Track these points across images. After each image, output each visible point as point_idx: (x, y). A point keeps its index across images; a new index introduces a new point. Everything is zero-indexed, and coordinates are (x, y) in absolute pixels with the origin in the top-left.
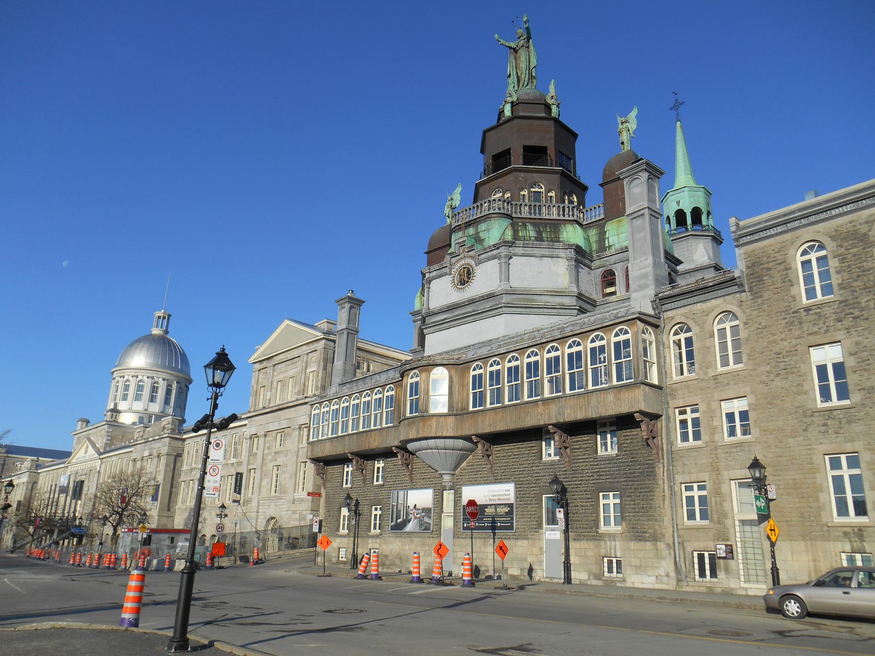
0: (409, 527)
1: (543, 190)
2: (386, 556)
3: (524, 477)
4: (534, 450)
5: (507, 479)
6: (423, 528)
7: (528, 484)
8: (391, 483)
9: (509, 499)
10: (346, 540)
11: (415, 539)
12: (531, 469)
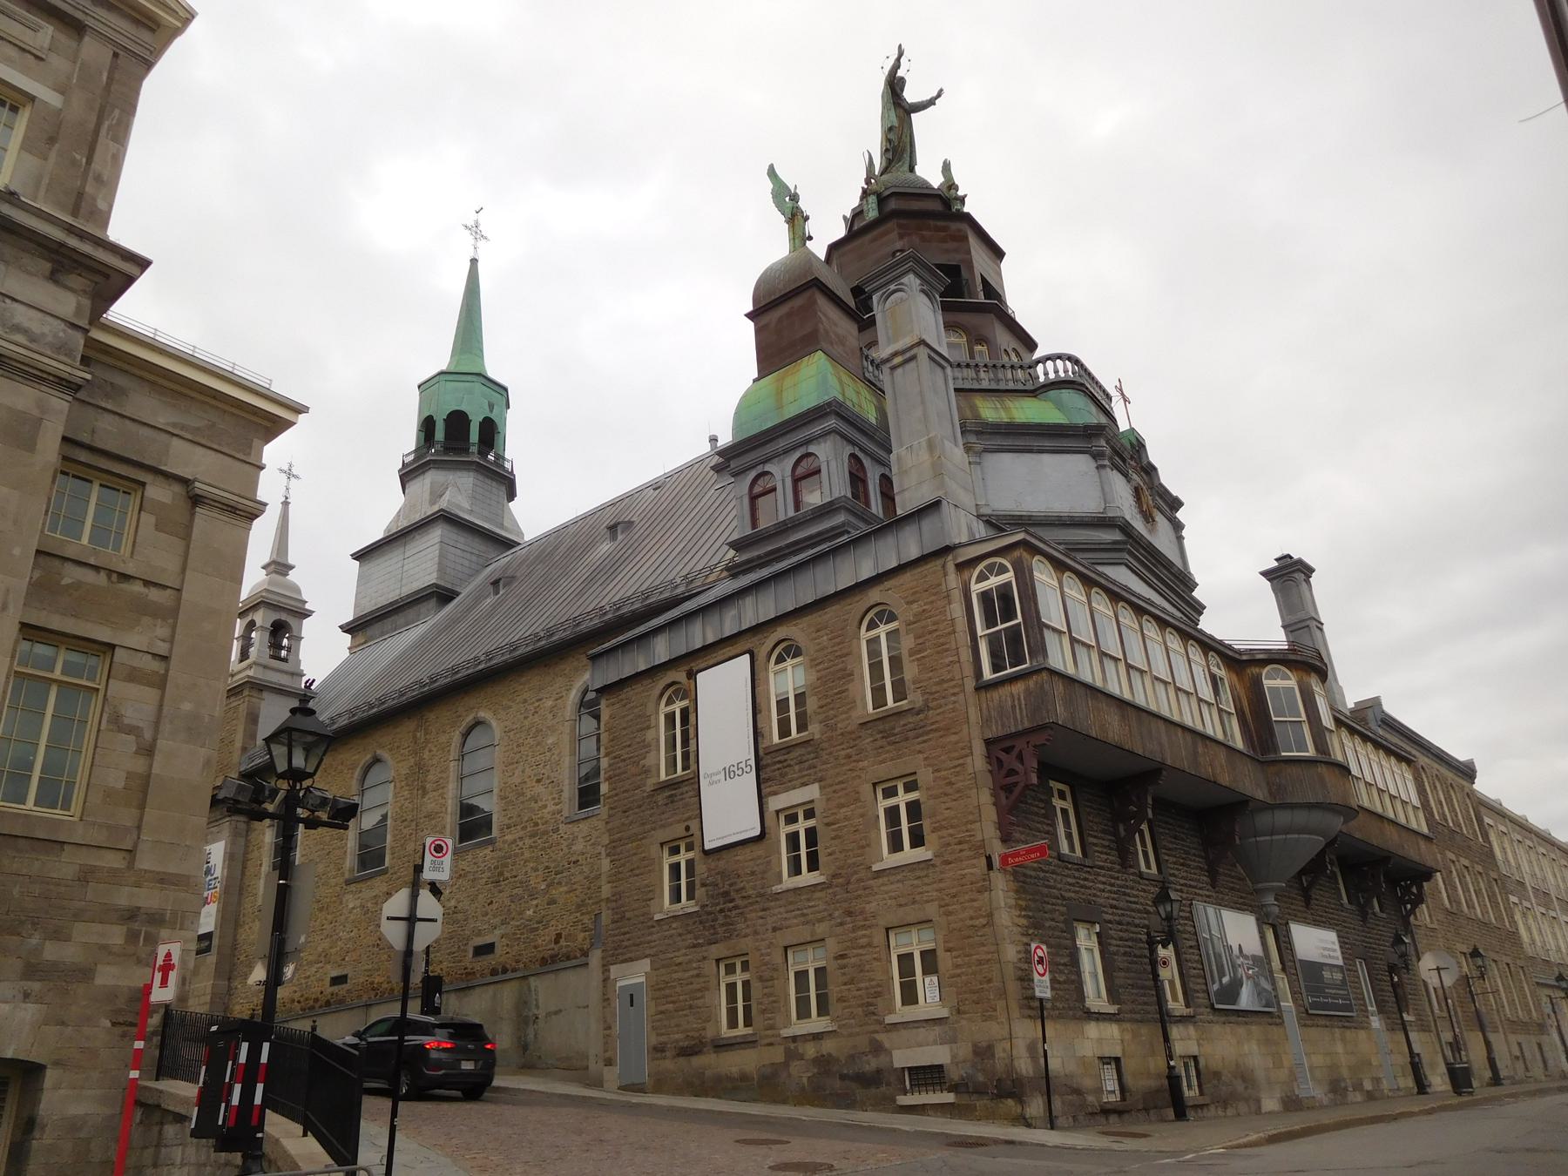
0: (1246, 1000)
2: (1217, 1075)
6: (1264, 1002)
8: (1182, 881)
10: (1113, 1030)
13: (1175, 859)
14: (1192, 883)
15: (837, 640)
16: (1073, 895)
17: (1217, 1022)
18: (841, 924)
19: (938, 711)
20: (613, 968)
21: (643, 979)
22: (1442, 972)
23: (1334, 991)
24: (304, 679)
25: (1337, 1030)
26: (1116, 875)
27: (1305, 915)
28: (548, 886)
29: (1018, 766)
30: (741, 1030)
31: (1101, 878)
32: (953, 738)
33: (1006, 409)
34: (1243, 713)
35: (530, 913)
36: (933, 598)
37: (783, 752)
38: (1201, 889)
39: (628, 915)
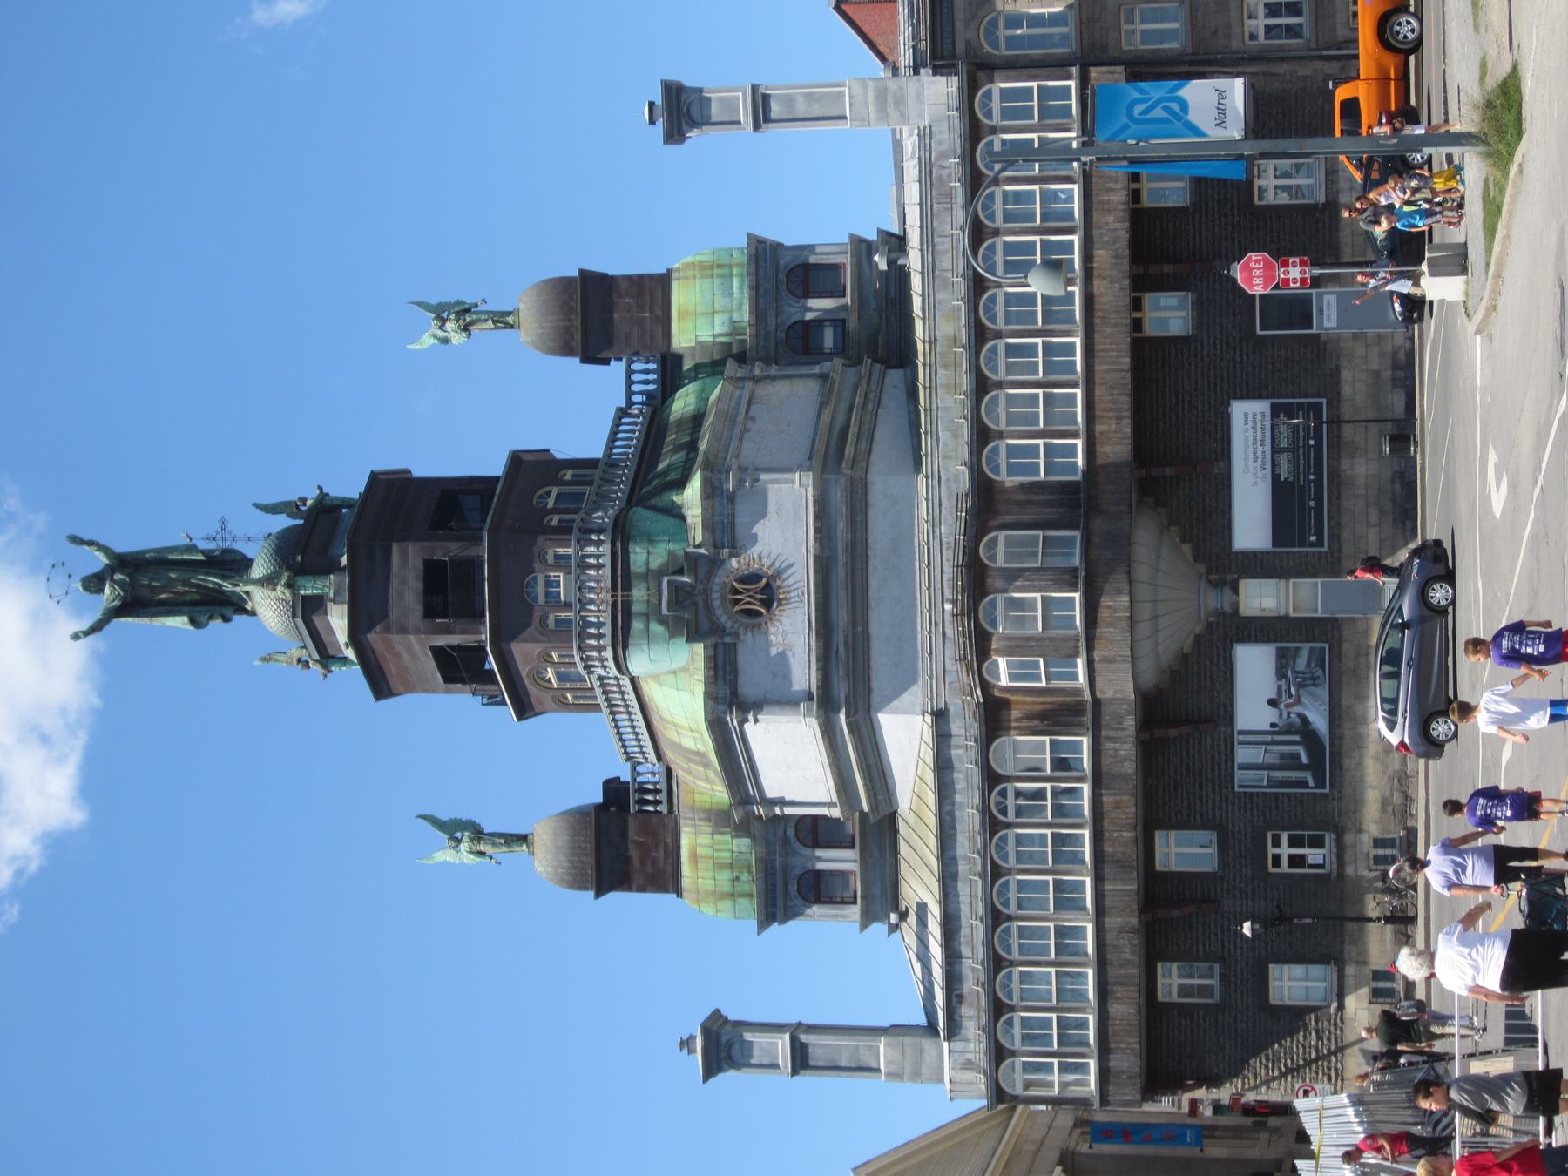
0: (1319, 721)
1: (555, 491)
3: (1222, 377)
4: (1169, 353)
5: (1222, 425)
6: (1320, 672)
7: (1234, 367)
8: (1218, 799)
9: (1263, 414)
11: (1345, 703)
12: (1206, 360)
13: (1198, 801)
23: (1301, 457)
25: (1343, 467)
31: (1232, 949)
38: (1219, 754)
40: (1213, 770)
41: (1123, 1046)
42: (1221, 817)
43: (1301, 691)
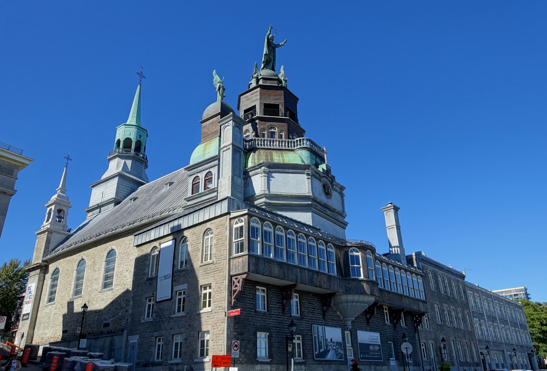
0: (330, 356)
6: (339, 357)
8: (309, 318)
10: (269, 367)
11: (332, 366)
13: (308, 311)
14: (314, 318)
15: (198, 238)
16: (259, 324)
17: (315, 364)
18: (187, 329)
19: (219, 264)
20: (129, 337)
21: (136, 341)
22: (408, 349)
23: (374, 353)
24: (68, 229)
25: (373, 366)
26: (280, 317)
27: (366, 328)
28: (126, 305)
29: (238, 284)
30: (160, 360)
31: (273, 318)
32: (222, 274)
33: (282, 156)
34: (339, 263)
35: (120, 314)
36: (223, 228)
37: (180, 272)
38: (318, 320)
39: (135, 320)
40: (314, 317)
41: (266, 269)
42: (305, 318)
43: (334, 350)
